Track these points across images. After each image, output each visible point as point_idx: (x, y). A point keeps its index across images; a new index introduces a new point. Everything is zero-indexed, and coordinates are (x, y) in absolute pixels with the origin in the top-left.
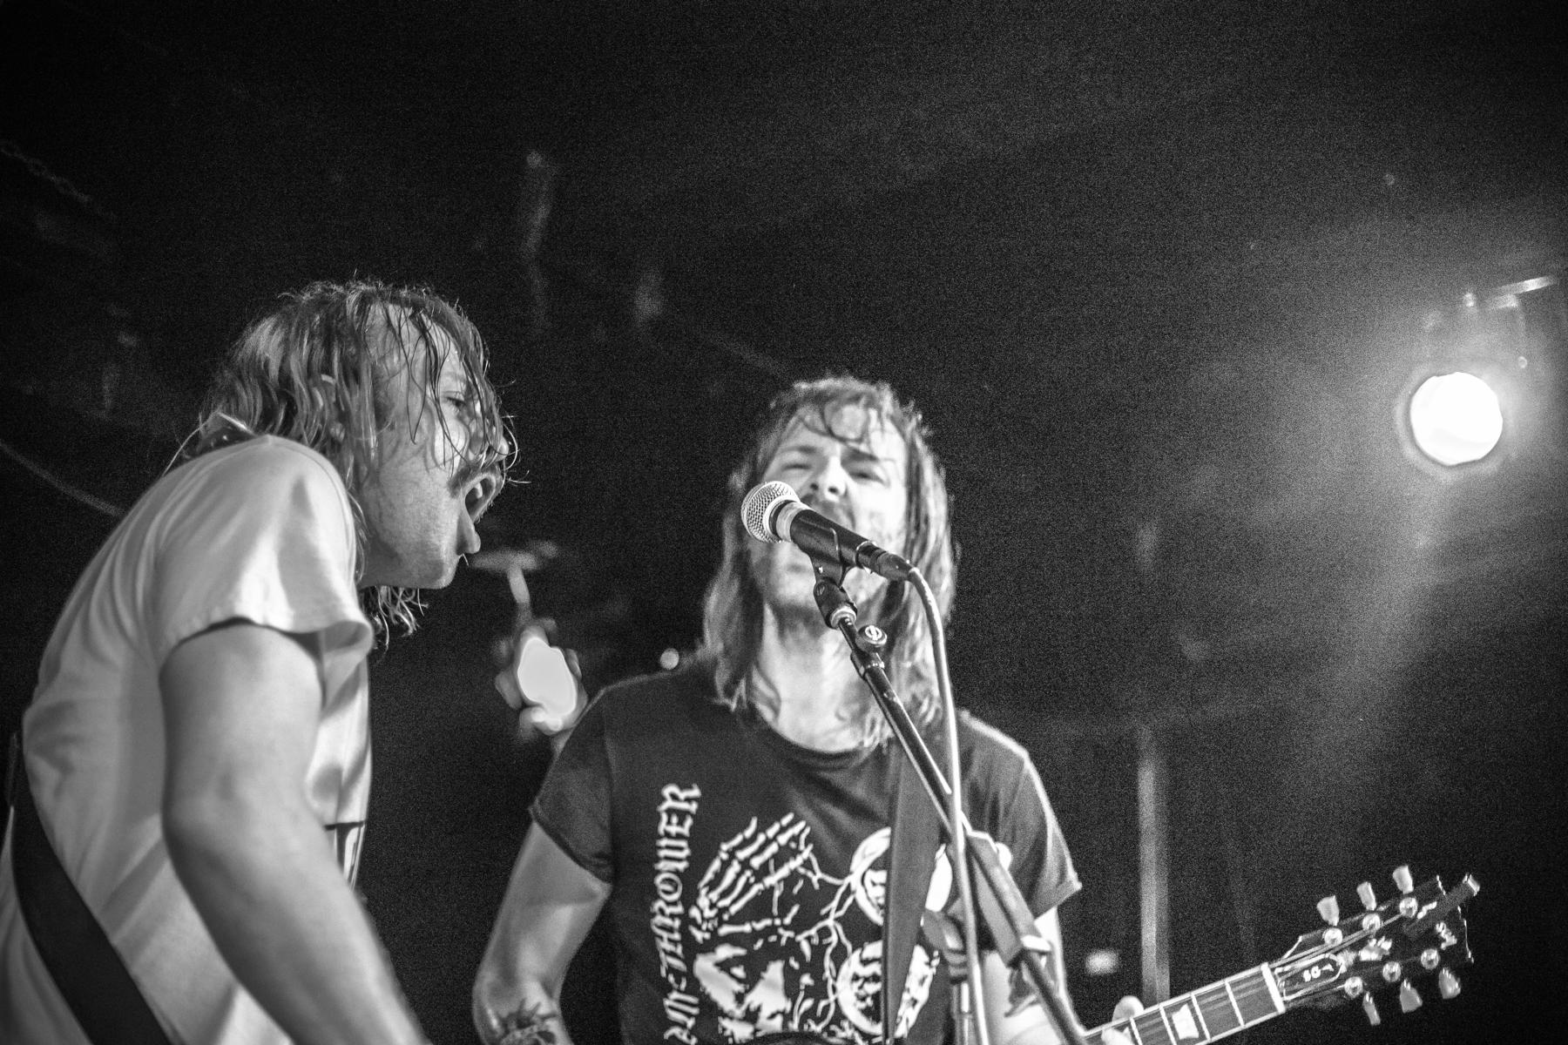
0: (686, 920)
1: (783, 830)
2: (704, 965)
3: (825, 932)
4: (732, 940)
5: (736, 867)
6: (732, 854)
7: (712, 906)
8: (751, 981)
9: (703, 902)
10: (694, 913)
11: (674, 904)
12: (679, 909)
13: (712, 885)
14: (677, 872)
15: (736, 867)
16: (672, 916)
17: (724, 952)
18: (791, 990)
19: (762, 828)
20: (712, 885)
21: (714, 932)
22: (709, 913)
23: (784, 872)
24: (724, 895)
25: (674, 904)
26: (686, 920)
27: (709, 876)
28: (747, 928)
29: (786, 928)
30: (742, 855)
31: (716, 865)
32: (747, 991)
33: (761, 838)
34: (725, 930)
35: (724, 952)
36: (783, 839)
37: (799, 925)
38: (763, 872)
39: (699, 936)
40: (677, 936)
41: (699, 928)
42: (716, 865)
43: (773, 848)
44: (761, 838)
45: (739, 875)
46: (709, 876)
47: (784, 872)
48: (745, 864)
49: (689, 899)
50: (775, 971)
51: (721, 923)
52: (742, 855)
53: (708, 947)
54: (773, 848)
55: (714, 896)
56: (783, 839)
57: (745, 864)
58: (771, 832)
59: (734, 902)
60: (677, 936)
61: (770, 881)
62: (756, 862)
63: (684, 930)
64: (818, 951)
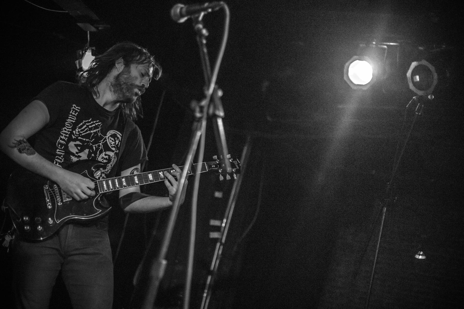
0: (72, 133)
1: (96, 123)
2: (72, 144)
3: (99, 146)
4: (80, 141)
5: (85, 126)
6: (85, 123)
7: (78, 132)
8: (81, 151)
9: (77, 130)
10: (74, 132)
11: (70, 129)
12: (71, 130)
13: (80, 128)
14: (72, 122)
15: (85, 126)
16: (68, 131)
17: (78, 143)
18: (89, 155)
19: (92, 120)
20: (80, 128)
21: (77, 137)
22: (77, 133)
23: (95, 131)
24: (81, 131)
25: (70, 129)
26: (72, 133)
27: (79, 125)
28: (84, 139)
29: (91, 143)
30: (87, 124)
31: (82, 124)
32: (79, 153)
33: (92, 122)
34: (79, 138)
35: (78, 143)
36: (96, 124)
37: (94, 143)
38: (91, 129)
39: (73, 137)
40: (68, 136)
41: (74, 135)
42: (82, 124)
43: (94, 125)
44: (92, 122)
45: (86, 128)
46: (79, 125)
47: (95, 131)
48: (88, 126)
49: (74, 129)
50: (87, 151)
51: (79, 136)
52: (87, 124)
53: (75, 140)
54: (94, 125)
55: (80, 130)
56: (96, 124)
57: (88, 126)
58: (94, 122)
59: (83, 133)
60: (68, 136)
61: (92, 132)
62: (90, 127)
63: (70, 135)
64: (97, 149)
